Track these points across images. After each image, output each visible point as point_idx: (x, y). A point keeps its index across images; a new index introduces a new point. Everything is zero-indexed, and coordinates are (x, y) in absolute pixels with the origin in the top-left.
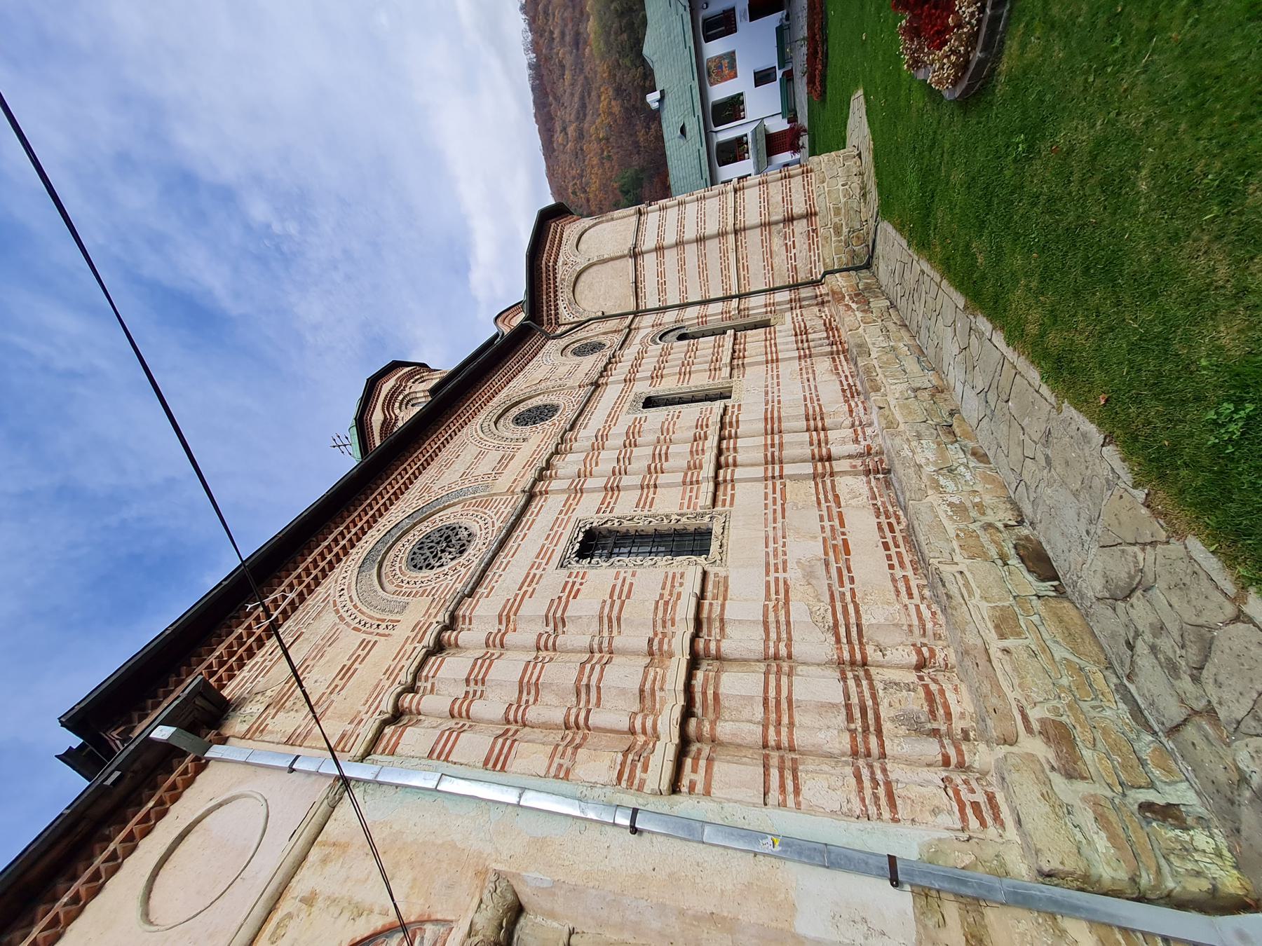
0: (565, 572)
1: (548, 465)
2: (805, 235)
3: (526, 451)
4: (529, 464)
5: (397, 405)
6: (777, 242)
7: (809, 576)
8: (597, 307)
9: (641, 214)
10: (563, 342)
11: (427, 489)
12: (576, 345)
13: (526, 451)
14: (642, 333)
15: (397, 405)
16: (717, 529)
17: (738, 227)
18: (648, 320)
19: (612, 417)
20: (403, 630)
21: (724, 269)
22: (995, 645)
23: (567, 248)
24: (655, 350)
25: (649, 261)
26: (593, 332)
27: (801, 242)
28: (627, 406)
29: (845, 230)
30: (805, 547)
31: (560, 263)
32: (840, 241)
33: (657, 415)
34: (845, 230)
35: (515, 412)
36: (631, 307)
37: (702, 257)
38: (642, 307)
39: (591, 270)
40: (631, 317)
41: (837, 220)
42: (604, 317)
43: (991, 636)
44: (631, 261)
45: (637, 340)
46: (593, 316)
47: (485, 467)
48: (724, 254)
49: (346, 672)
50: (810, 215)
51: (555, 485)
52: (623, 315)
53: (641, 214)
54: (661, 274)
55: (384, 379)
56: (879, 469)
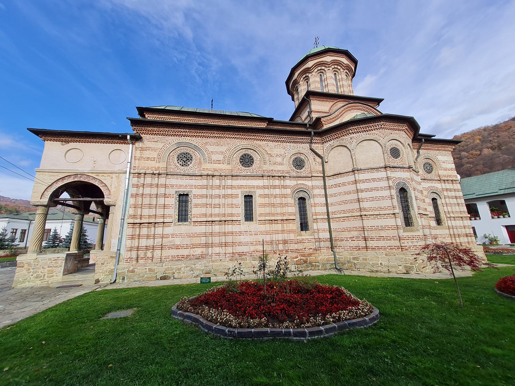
0: (174, 193)
1: (213, 176)
2: (358, 245)
4: (215, 170)
5: (319, 68)
6: (355, 234)
7: (170, 242)
9: (385, 168)
11: (206, 144)
12: (303, 157)
15: (319, 68)
16: (185, 223)
17: (363, 216)
19: (240, 187)
20: (157, 165)
21: (344, 212)
22: (147, 268)
23: (364, 135)
24: (289, 191)
25: (351, 178)
27: (355, 243)
28: (248, 190)
29: (356, 262)
30: (178, 241)
31: (352, 136)
32: (350, 259)
33: (240, 201)
34: (356, 262)
35: (249, 152)
37: (351, 202)
39: (348, 151)
41: (361, 258)
43: (149, 267)
44: (351, 170)
45: (299, 182)
47: (214, 157)
48: (352, 211)
49: (148, 159)
50: (367, 248)
53: (385, 168)
54: (344, 184)
55: (332, 54)
56: (202, 257)
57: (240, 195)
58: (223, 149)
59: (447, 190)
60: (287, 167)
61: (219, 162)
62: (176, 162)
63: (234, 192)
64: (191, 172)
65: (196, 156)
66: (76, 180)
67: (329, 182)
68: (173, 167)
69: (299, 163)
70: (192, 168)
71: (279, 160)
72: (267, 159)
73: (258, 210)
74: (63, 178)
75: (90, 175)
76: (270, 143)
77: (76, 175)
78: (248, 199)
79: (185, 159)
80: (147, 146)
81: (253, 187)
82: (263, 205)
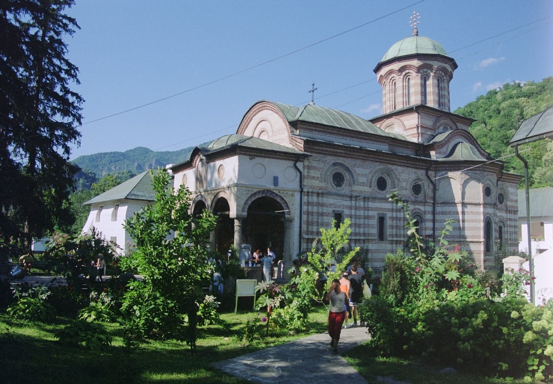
3: (367, 189)
8: (440, 186)
10: (424, 177)
11: (355, 166)
13: (367, 189)
14: (422, 208)
18: (429, 209)
26: (427, 189)
33: (375, 222)
36: (439, 200)
38: (436, 205)
40: (433, 202)
42: (435, 190)
45: (417, 207)
46: (437, 186)
47: (362, 179)
51: (353, 202)
52: (434, 198)
57: (376, 217)
58: (367, 171)
59: (510, 220)
60: (407, 193)
61: (363, 184)
62: (332, 182)
63: (371, 213)
64: (343, 192)
65: (347, 176)
66: (264, 195)
67: (438, 209)
68: (331, 187)
69: (417, 189)
70: (345, 189)
71: (404, 184)
72: (396, 183)
73: (388, 231)
74: (255, 194)
75: (274, 191)
76: (399, 168)
77: (263, 191)
78: (382, 220)
79: (338, 179)
80: (312, 165)
81: (385, 209)
82: (392, 227)
